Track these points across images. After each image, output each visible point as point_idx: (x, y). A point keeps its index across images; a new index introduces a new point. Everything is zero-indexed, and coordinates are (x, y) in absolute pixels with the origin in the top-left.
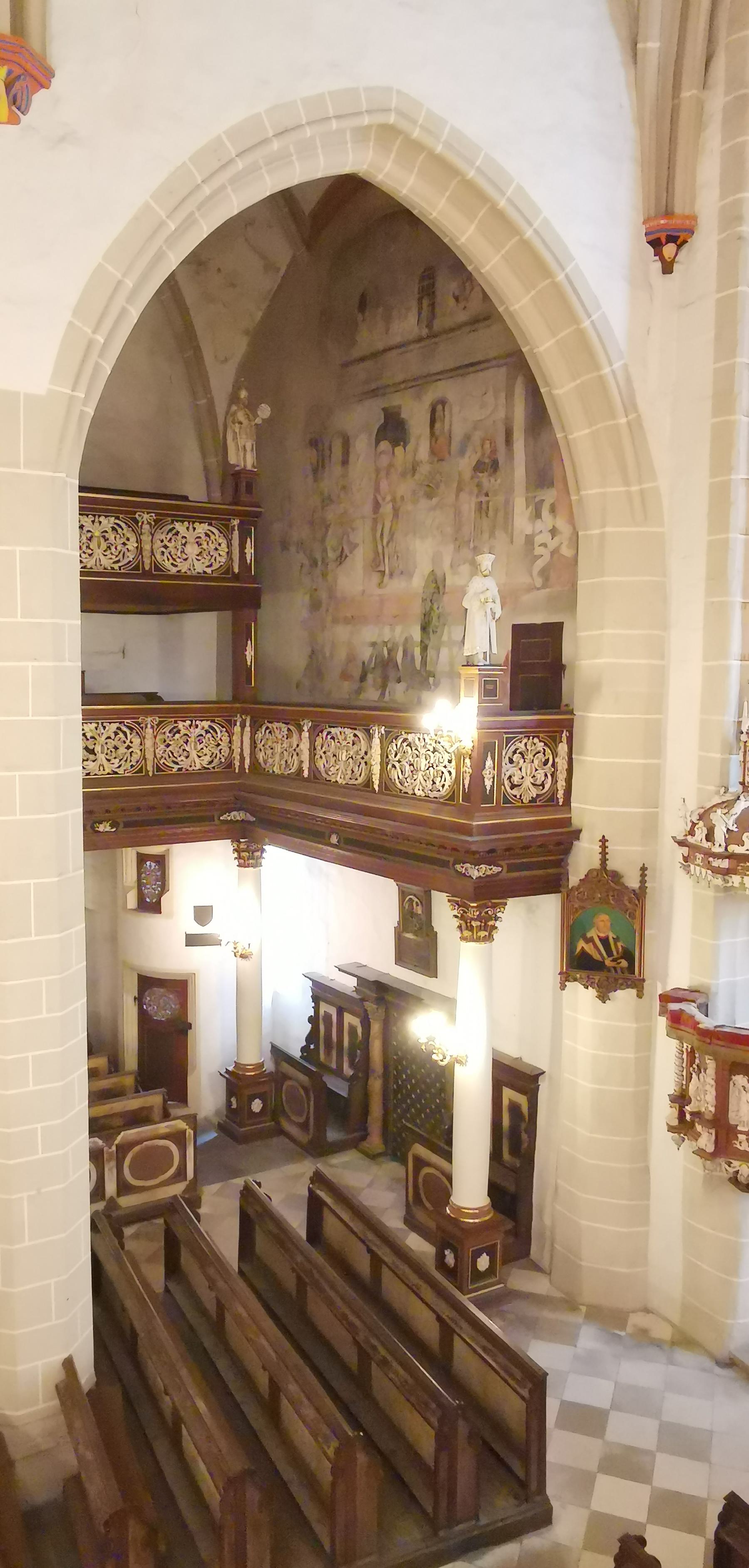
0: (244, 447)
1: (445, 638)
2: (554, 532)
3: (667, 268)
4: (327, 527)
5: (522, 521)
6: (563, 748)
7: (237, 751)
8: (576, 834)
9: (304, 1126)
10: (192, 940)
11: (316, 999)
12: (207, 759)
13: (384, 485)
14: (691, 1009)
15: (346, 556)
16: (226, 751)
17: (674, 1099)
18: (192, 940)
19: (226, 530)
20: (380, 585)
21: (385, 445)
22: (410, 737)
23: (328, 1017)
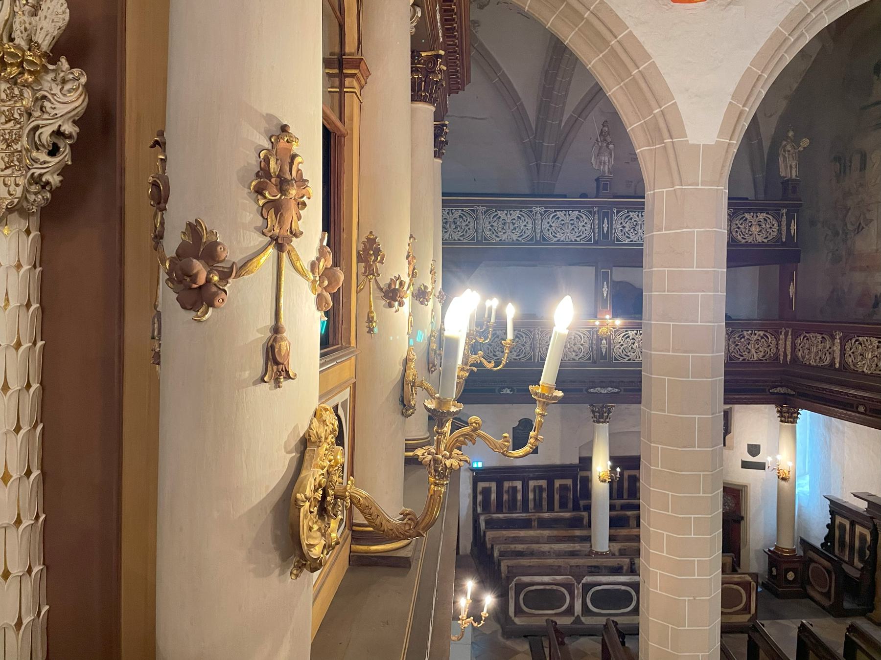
0: (791, 167)
4: (848, 210)
7: (782, 350)
9: (827, 595)
10: (745, 465)
11: (832, 513)
12: (762, 354)
15: (863, 228)
16: (774, 350)
18: (745, 465)
19: (778, 217)
23: (842, 527)
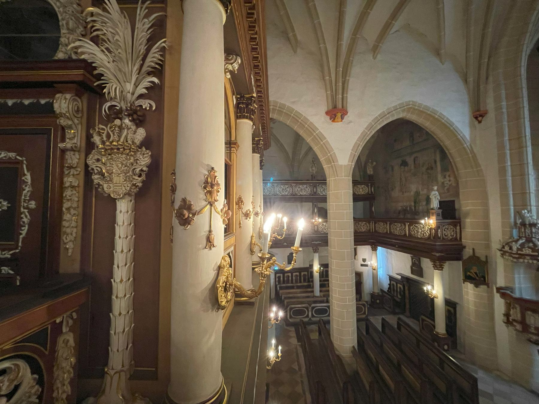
0: (371, 171)
1: (421, 204)
2: (450, 181)
3: (480, 122)
5: (440, 178)
6: (458, 228)
7: (371, 228)
8: (465, 247)
9: (390, 308)
10: (362, 265)
11: (390, 280)
12: (365, 229)
13: (402, 175)
14: (508, 292)
16: (369, 228)
17: (504, 315)
18: (362, 265)
20: (403, 194)
21: (402, 167)
22: (416, 225)
23: (393, 285)
